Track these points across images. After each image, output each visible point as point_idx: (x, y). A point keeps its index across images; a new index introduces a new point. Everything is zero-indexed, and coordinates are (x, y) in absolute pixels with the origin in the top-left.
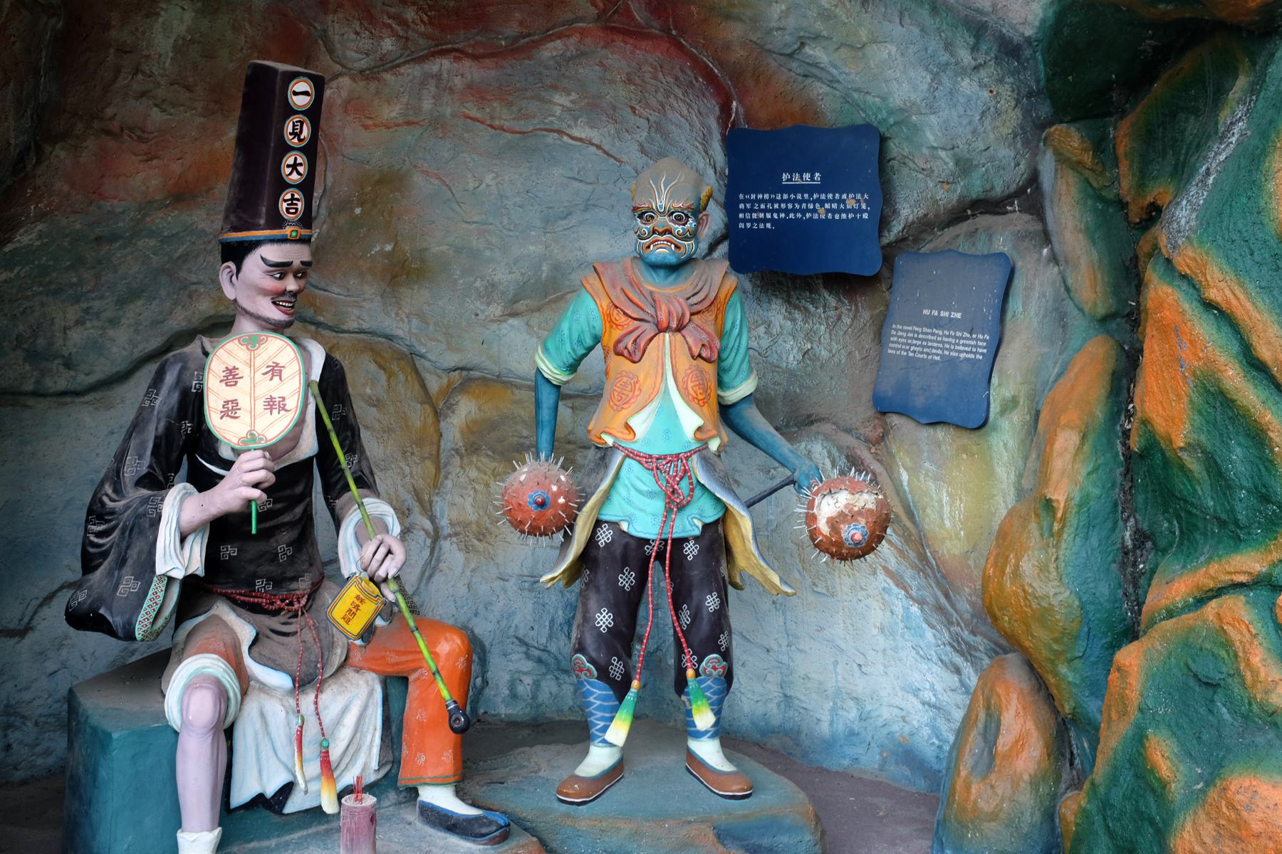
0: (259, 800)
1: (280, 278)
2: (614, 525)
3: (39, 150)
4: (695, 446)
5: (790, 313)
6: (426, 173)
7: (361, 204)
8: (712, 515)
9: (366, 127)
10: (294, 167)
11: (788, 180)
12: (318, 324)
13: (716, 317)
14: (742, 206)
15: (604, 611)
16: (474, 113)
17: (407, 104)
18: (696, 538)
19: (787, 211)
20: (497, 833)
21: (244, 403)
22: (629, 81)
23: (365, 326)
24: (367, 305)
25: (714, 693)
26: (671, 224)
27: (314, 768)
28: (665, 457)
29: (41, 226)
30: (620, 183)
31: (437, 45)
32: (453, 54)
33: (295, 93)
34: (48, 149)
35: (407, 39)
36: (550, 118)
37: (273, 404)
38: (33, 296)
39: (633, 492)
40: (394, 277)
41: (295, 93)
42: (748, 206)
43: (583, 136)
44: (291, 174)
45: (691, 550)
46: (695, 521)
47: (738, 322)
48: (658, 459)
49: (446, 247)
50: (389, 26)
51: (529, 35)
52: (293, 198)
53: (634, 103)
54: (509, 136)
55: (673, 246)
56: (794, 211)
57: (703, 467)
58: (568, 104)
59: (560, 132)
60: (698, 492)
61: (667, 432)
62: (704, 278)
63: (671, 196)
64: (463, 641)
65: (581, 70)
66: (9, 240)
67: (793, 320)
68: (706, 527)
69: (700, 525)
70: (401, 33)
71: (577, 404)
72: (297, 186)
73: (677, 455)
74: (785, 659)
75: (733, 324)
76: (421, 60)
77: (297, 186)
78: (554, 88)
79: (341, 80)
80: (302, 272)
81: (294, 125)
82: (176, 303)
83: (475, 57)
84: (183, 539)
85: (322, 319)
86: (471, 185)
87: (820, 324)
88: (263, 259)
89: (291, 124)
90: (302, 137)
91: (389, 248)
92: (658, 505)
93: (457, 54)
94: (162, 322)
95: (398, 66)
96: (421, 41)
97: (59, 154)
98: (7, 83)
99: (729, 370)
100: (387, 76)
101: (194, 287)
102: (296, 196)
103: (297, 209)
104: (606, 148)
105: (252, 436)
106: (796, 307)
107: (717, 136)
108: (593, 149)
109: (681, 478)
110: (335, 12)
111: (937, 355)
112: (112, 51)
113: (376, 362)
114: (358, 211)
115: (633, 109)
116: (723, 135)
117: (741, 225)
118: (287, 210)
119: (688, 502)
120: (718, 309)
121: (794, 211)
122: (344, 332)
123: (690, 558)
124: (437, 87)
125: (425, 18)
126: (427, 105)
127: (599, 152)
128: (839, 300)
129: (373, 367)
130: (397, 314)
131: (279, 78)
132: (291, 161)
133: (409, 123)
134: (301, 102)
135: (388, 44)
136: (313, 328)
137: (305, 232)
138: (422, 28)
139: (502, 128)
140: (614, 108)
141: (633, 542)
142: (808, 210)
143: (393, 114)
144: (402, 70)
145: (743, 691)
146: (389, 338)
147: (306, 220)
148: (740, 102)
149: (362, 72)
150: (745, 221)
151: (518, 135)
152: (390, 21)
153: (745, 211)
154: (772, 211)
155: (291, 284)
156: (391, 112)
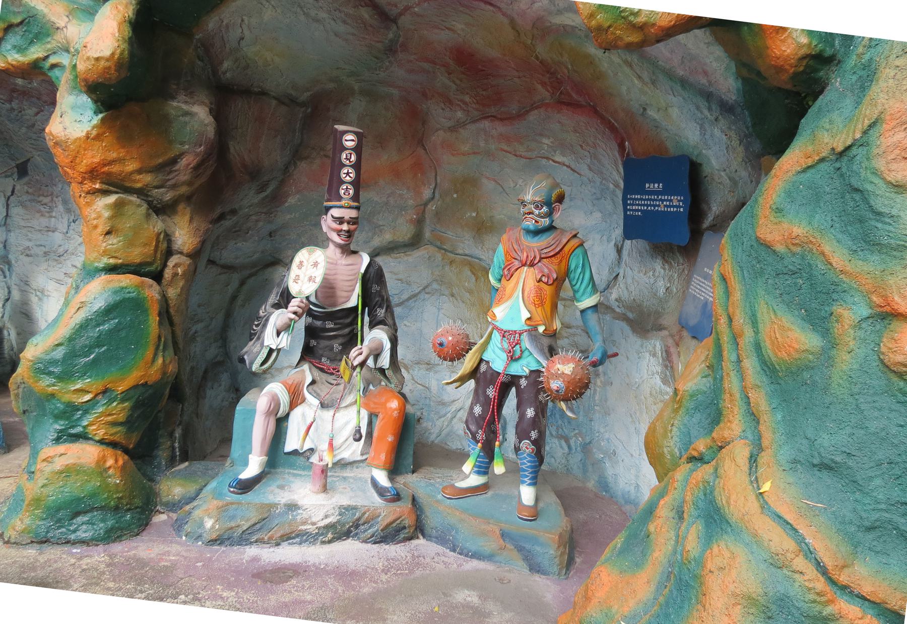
0: (295, 452)
1: (339, 224)
2: (488, 362)
3: (295, 164)
4: (526, 328)
5: (664, 265)
6: (488, 178)
7: (457, 192)
8: (534, 367)
9: (453, 155)
10: (348, 174)
11: (649, 188)
12: (444, 249)
13: (561, 261)
14: (629, 202)
15: (478, 405)
16: (506, 148)
17: (472, 144)
18: (526, 377)
19: (647, 206)
20: (389, 497)
21: (301, 277)
22: (575, 131)
23: (467, 252)
24: (467, 242)
25: (528, 462)
26: (533, 209)
27: (325, 446)
28: (509, 331)
29: (298, 196)
30: (583, 186)
31: (483, 114)
32: (490, 118)
33: (346, 140)
34: (298, 163)
35: (468, 111)
36: (543, 151)
37: (311, 279)
38: (305, 226)
39: (496, 349)
40: (479, 230)
41: (346, 140)
42: (631, 202)
43: (560, 160)
44: (346, 177)
45: (523, 383)
46: (524, 368)
47: (581, 265)
48: (505, 332)
49: (503, 216)
50: (459, 105)
51: (524, 108)
52: (347, 188)
53: (581, 143)
54: (525, 160)
55: (534, 221)
56: (651, 205)
57: (529, 339)
58: (551, 144)
59: (548, 158)
60: (526, 353)
61: (512, 319)
62: (556, 239)
63: (534, 195)
64: (399, 404)
65: (551, 126)
66: (286, 201)
67: (664, 269)
68: (532, 372)
69: (527, 371)
70: (465, 109)
71: (567, 304)
72: (349, 183)
73: (515, 331)
74: (637, 462)
75: (576, 267)
76: (474, 122)
77: (349, 183)
78: (541, 135)
79: (439, 132)
80: (354, 221)
81: (346, 155)
82: (374, 234)
83: (501, 120)
84: (278, 334)
85: (445, 247)
86: (512, 185)
87: (676, 273)
88: (332, 216)
89: (345, 155)
90: (351, 160)
91: (474, 214)
92: (504, 356)
93: (493, 118)
94: (369, 242)
95: (466, 125)
96: (476, 113)
97: (303, 165)
98: (276, 136)
99: (578, 291)
100: (460, 130)
101: (382, 227)
102: (349, 187)
103: (349, 193)
104: (573, 167)
105: (300, 292)
106: (667, 262)
107: (620, 162)
108: (565, 167)
109: (517, 344)
110: (431, 99)
111: (703, 296)
112: (331, 120)
113: (471, 270)
114: (455, 196)
115: (581, 146)
116: (622, 161)
117: (628, 213)
118: (344, 193)
119: (520, 358)
120: (562, 257)
121: (651, 205)
122: (457, 254)
123: (522, 387)
124: (485, 135)
125: (475, 101)
126: (482, 144)
127: (569, 170)
128: (684, 260)
129: (469, 273)
130: (482, 248)
131: (338, 133)
132: (346, 171)
133: (474, 153)
134: (350, 144)
135: (460, 114)
136: (443, 251)
137: (356, 204)
138: (474, 106)
139: (521, 156)
140: (572, 146)
141: (495, 373)
142: (656, 205)
143: (466, 149)
144: (467, 127)
145: (621, 476)
146: (480, 259)
147: (356, 198)
148: (629, 143)
149: (449, 128)
150: (630, 210)
151: (528, 160)
152: (459, 103)
153: (630, 205)
154: (641, 205)
155: (345, 227)
156: (465, 148)
